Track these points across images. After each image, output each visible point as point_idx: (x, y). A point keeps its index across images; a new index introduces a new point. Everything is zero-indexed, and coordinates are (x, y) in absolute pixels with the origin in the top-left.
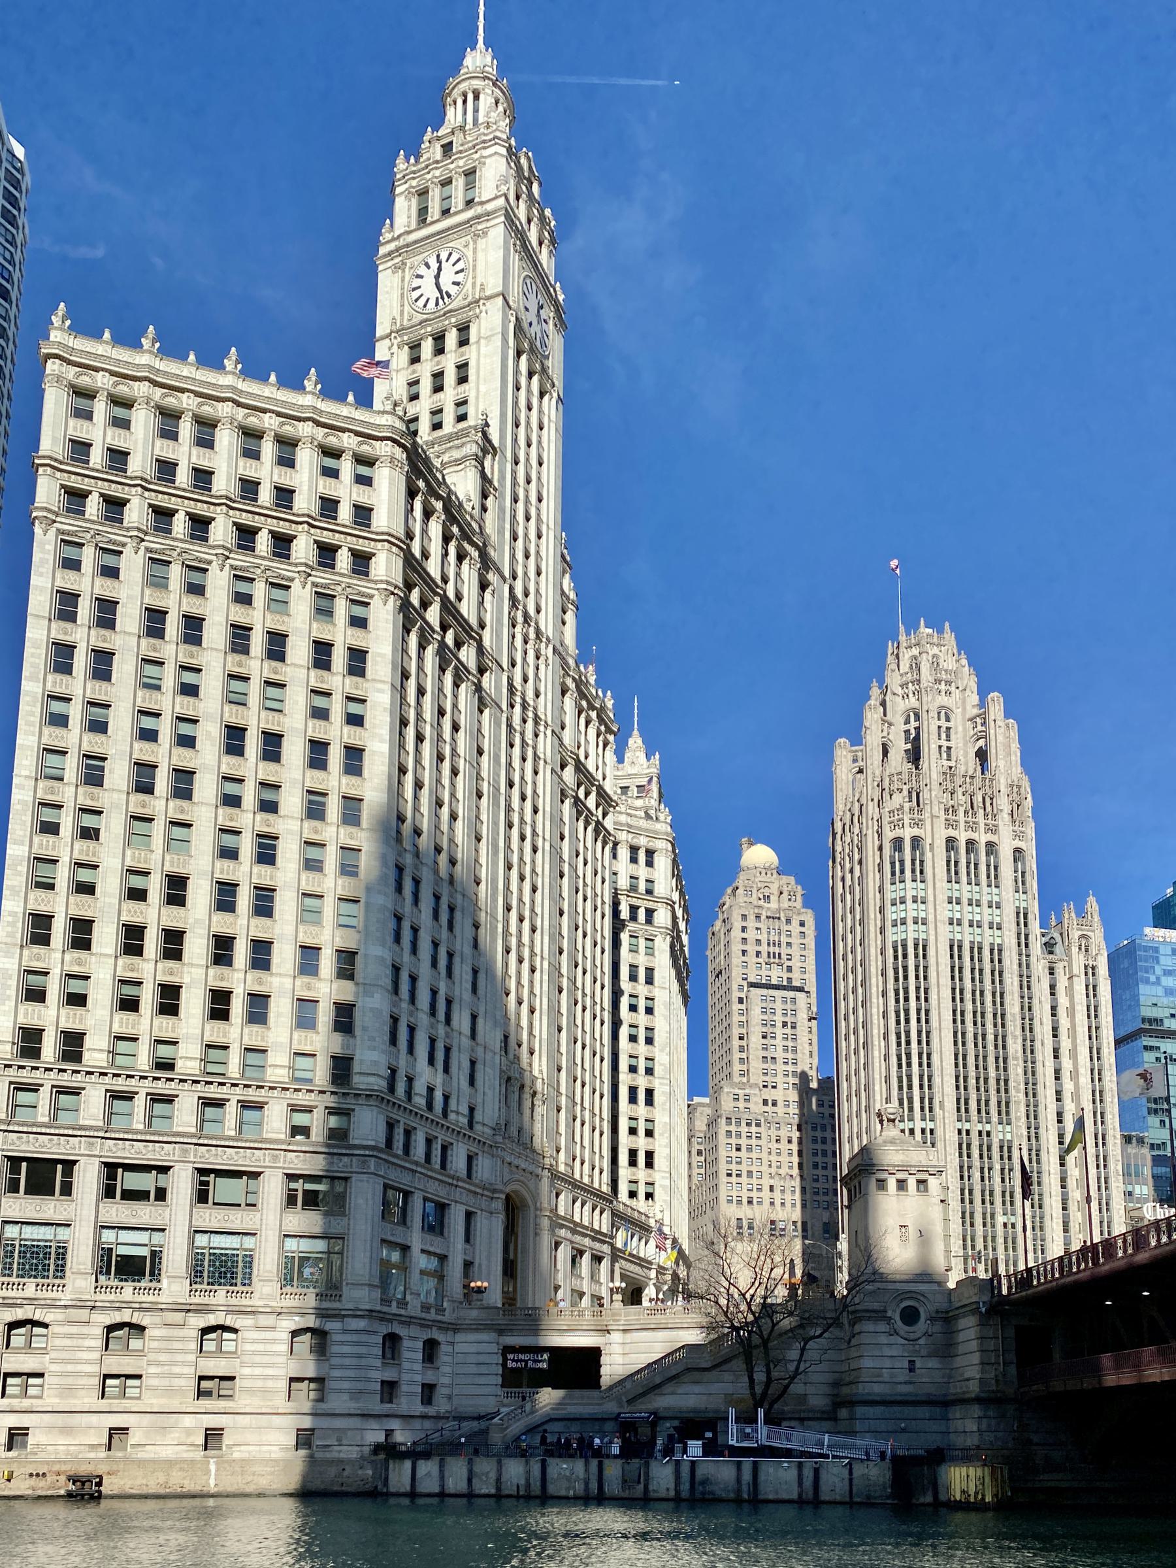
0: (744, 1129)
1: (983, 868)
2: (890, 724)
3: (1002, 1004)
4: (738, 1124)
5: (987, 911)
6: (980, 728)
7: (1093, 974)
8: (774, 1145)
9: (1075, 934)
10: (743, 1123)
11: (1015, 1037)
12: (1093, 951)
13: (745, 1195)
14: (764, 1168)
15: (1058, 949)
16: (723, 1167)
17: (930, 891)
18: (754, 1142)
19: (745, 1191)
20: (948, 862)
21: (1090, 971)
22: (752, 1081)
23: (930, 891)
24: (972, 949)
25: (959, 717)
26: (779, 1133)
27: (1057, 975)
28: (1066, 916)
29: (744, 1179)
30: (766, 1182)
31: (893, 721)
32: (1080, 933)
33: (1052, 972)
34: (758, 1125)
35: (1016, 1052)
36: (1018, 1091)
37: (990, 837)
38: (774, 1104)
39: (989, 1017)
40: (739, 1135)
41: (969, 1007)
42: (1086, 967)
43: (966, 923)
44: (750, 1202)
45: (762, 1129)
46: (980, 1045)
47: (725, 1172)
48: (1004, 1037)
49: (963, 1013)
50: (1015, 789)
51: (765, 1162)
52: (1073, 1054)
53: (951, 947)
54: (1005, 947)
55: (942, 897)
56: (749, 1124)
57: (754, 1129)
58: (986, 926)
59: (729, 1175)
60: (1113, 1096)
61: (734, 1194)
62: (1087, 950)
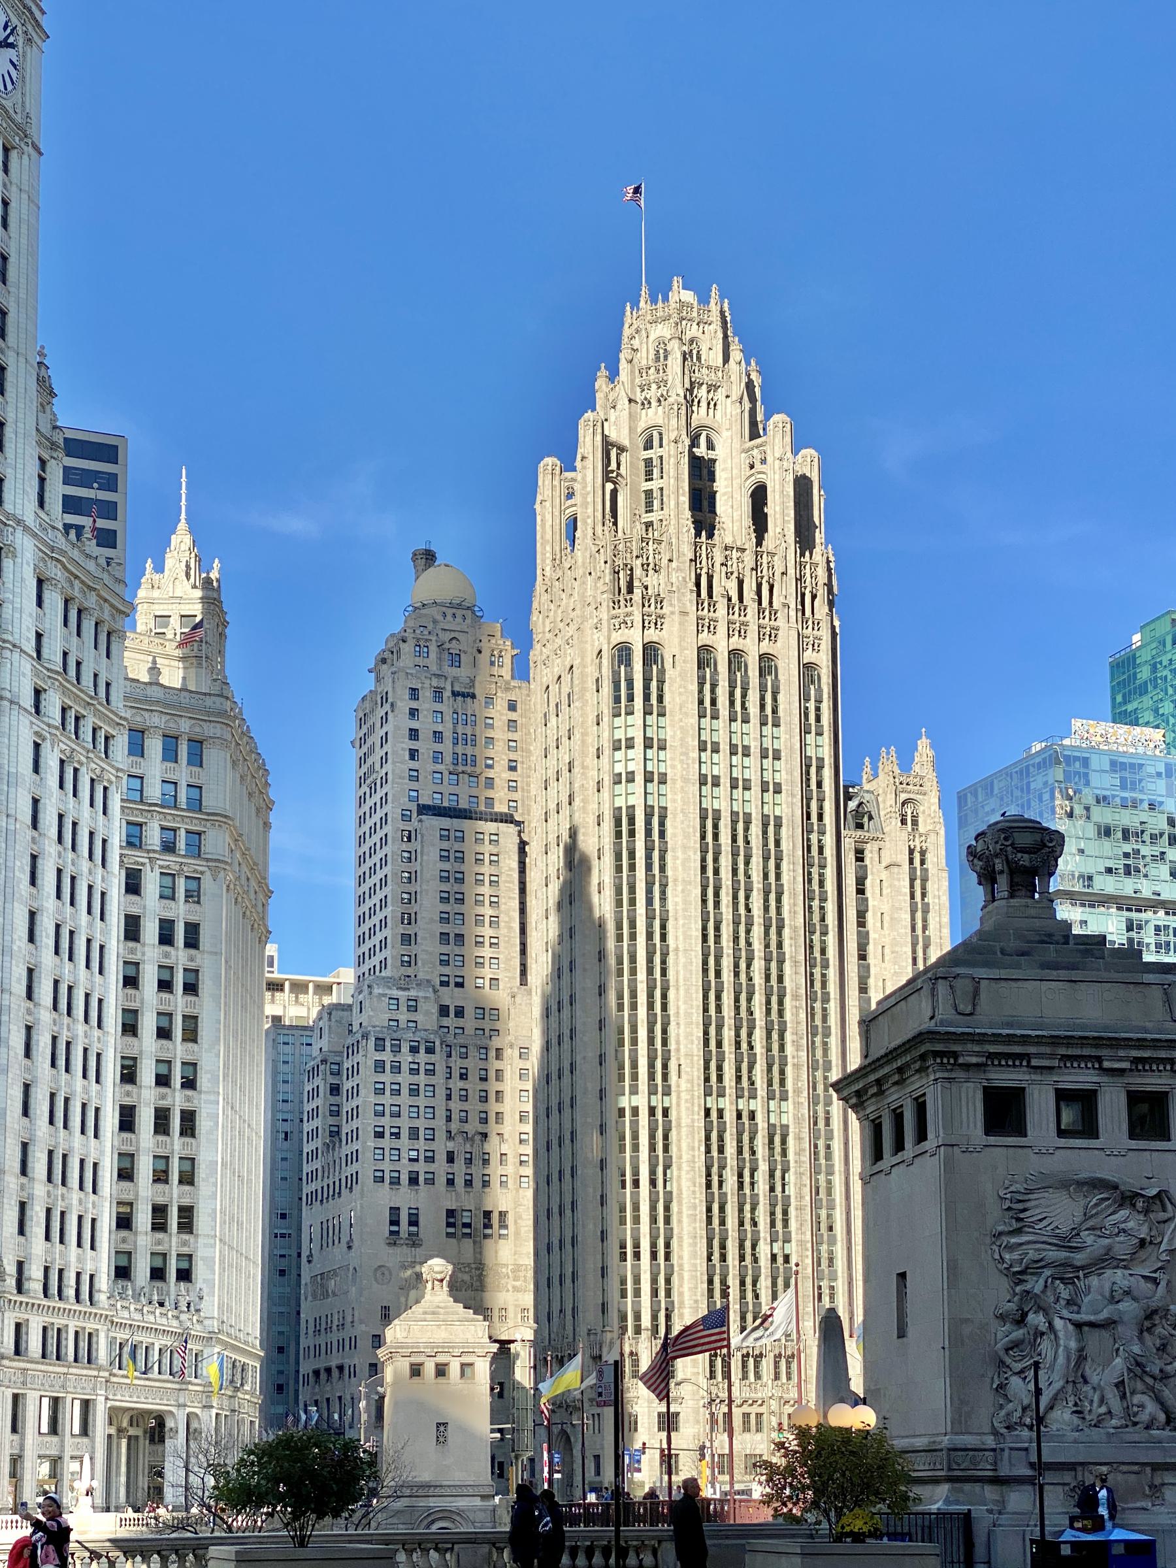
0: (406, 1057)
4: (397, 1049)
5: (753, 775)
8: (457, 1084)
10: (405, 1048)
13: (405, 1168)
14: (440, 1123)
16: (366, 1123)
18: (422, 1079)
19: (405, 1161)
22: (421, 976)
26: (465, 1063)
29: (405, 1141)
30: (441, 1146)
34: (430, 1051)
37: (766, 646)
38: (460, 1012)
40: (397, 1069)
44: (414, 1180)
45: (438, 1058)
47: (371, 1130)
51: (441, 1113)
56: (414, 1050)
57: (422, 1057)
59: (380, 1135)
61: (386, 1166)
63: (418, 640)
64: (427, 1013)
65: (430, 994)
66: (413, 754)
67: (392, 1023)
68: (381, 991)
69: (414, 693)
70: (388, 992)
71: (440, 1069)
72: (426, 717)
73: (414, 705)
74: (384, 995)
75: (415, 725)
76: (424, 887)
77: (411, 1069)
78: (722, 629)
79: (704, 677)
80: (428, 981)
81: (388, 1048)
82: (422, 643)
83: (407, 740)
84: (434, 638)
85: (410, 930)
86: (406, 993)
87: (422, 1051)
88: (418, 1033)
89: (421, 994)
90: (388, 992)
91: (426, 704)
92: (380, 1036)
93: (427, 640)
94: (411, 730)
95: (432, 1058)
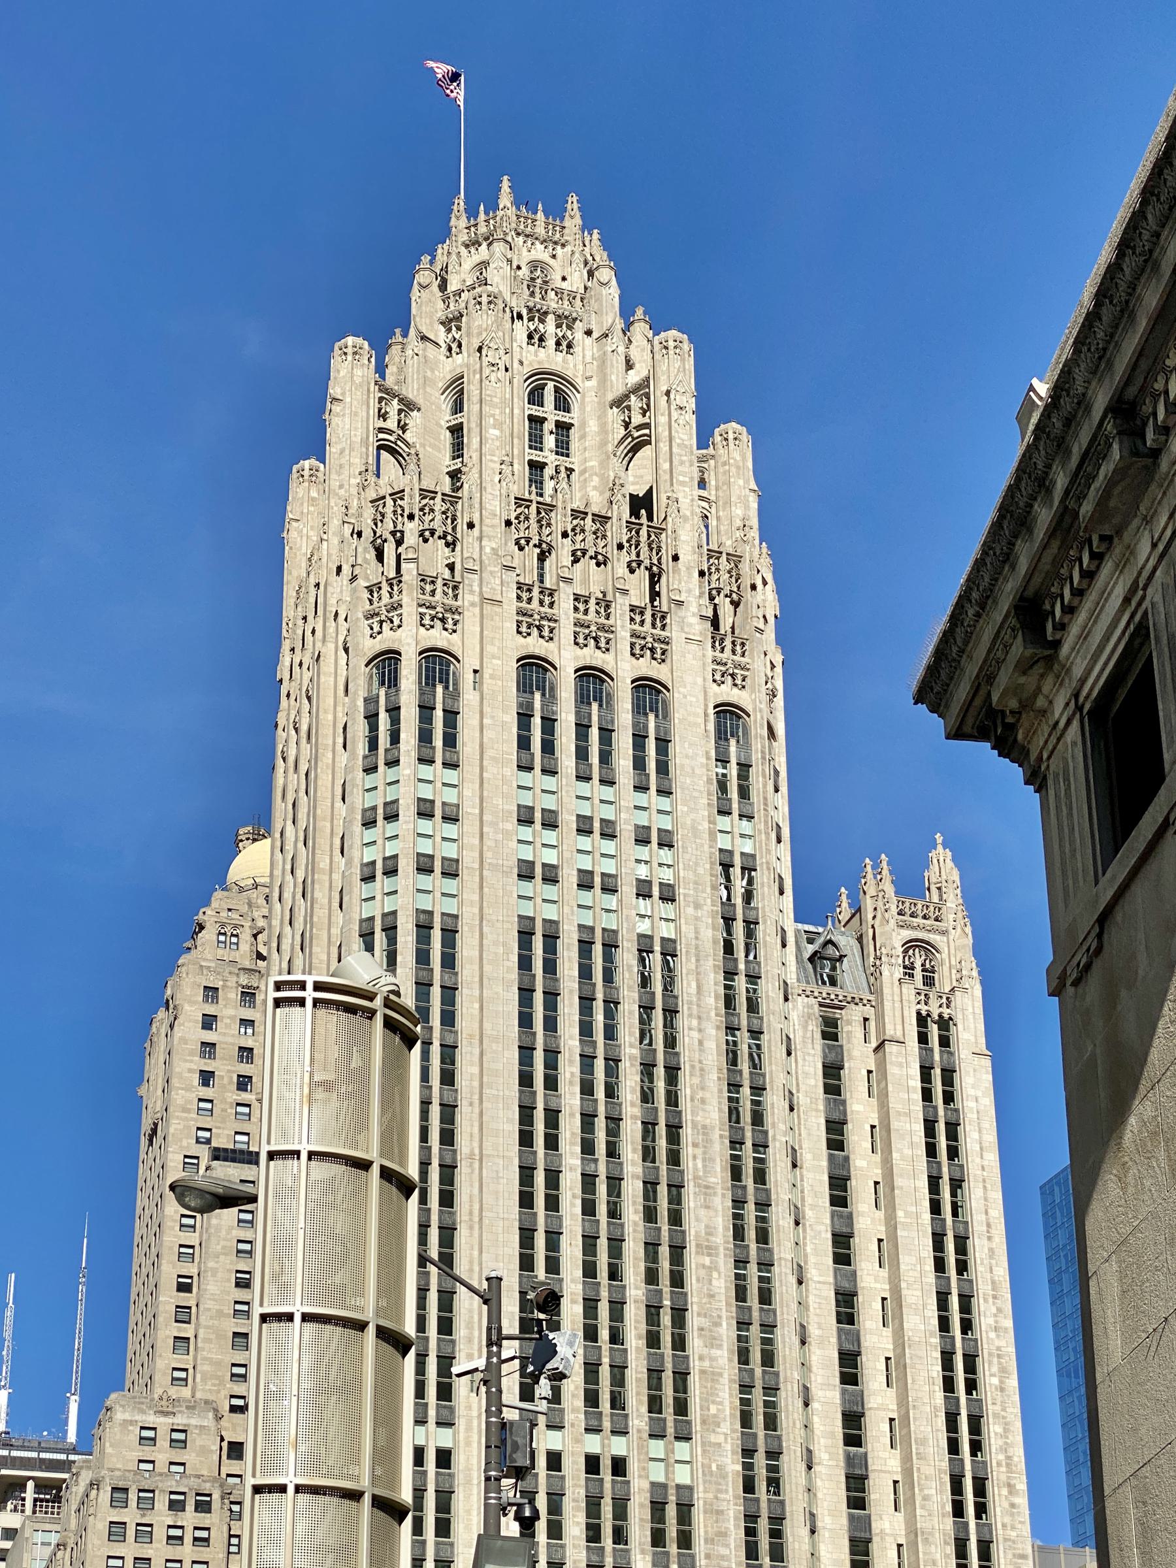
0: (161, 1517)
1: (623, 743)
2: (408, 406)
3: (672, 1099)
6: (637, 419)
7: (945, 1042)
9: (894, 938)
10: (162, 1503)
11: (707, 1190)
12: (944, 982)
15: (851, 973)
17: (470, 792)
20: (524, 718)
21: (934, 1032)
23: (470, 792)
24: (585, 946)
25: (591, 399)
27: (843, 1039)
28: (871, 890)
31: (420, 401)
32: (908, 934)
33: (830, 1031)
34: (203, 1507)
35: (710, 1231)
36: (712, 1342)
37: (646, 667)
39: (631, 1130)
40: (145, 1532)
41: (570, 1099)
42: (922, 1020)
43: (569, 878)
45: (216, 1520)
46: (602, 1209)
48: (676, 1188)
49: (552, 1117)
50: (724, 564)
52: (888, 1253)
53: (525, 936)
54: (681, 949)
55: (506, 805)
56: (176, 1506)
57: (190, 1518)
58: (628, 889)
60: (1003, 1370)
62: (929, 981)
63: (223, 925)
64: (204, 1451)
65: (209, 1420)
66: (206, 1077)
67: (143, 1466)
68: (127, 1416)
69: (211, 993)
70: (138, 1417)
71: (218, 1537)
72: (228, 1026)
73: (210, 1009)
74: (132, 1422)
75: (209, 1036)
76: (211, 1264)
77: (169, 1538)
78: (566, 630)
79: (530, 705)
80: (206, 1402)
81: (133, 1502)
82: (228, 930)
83: (197, 1058)
84: (247, 924)
85: (188, 1331)
86: (169, 1420)
87: (190, 1506)
88: (185, 1481)
89: (193, 1422)
90: (138, 1417)
91: (229, 1009)
92: (121, 1484)
93: (235, 927)
94: (204, 1044)
95: (204, 1519)
